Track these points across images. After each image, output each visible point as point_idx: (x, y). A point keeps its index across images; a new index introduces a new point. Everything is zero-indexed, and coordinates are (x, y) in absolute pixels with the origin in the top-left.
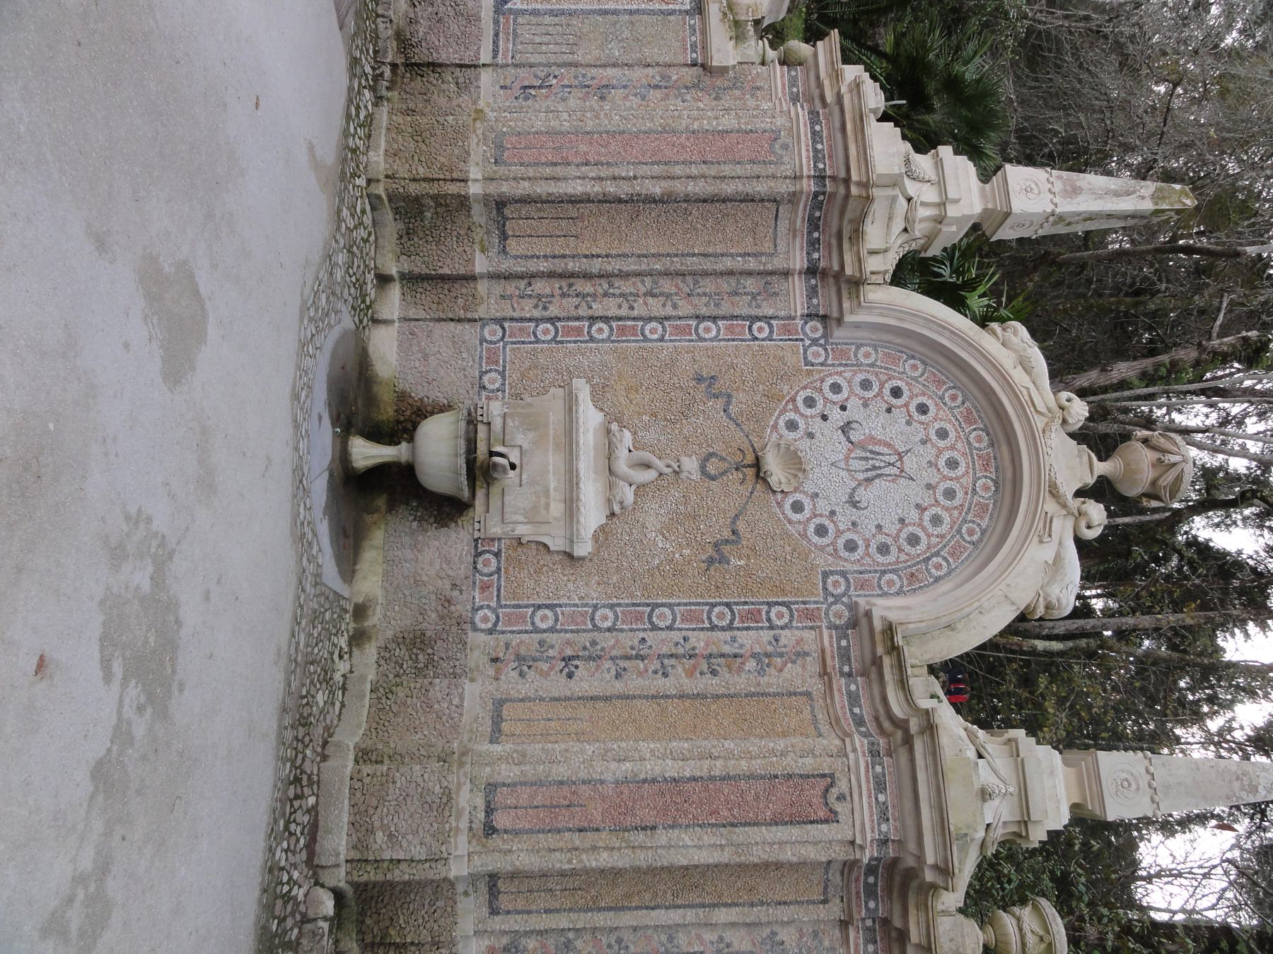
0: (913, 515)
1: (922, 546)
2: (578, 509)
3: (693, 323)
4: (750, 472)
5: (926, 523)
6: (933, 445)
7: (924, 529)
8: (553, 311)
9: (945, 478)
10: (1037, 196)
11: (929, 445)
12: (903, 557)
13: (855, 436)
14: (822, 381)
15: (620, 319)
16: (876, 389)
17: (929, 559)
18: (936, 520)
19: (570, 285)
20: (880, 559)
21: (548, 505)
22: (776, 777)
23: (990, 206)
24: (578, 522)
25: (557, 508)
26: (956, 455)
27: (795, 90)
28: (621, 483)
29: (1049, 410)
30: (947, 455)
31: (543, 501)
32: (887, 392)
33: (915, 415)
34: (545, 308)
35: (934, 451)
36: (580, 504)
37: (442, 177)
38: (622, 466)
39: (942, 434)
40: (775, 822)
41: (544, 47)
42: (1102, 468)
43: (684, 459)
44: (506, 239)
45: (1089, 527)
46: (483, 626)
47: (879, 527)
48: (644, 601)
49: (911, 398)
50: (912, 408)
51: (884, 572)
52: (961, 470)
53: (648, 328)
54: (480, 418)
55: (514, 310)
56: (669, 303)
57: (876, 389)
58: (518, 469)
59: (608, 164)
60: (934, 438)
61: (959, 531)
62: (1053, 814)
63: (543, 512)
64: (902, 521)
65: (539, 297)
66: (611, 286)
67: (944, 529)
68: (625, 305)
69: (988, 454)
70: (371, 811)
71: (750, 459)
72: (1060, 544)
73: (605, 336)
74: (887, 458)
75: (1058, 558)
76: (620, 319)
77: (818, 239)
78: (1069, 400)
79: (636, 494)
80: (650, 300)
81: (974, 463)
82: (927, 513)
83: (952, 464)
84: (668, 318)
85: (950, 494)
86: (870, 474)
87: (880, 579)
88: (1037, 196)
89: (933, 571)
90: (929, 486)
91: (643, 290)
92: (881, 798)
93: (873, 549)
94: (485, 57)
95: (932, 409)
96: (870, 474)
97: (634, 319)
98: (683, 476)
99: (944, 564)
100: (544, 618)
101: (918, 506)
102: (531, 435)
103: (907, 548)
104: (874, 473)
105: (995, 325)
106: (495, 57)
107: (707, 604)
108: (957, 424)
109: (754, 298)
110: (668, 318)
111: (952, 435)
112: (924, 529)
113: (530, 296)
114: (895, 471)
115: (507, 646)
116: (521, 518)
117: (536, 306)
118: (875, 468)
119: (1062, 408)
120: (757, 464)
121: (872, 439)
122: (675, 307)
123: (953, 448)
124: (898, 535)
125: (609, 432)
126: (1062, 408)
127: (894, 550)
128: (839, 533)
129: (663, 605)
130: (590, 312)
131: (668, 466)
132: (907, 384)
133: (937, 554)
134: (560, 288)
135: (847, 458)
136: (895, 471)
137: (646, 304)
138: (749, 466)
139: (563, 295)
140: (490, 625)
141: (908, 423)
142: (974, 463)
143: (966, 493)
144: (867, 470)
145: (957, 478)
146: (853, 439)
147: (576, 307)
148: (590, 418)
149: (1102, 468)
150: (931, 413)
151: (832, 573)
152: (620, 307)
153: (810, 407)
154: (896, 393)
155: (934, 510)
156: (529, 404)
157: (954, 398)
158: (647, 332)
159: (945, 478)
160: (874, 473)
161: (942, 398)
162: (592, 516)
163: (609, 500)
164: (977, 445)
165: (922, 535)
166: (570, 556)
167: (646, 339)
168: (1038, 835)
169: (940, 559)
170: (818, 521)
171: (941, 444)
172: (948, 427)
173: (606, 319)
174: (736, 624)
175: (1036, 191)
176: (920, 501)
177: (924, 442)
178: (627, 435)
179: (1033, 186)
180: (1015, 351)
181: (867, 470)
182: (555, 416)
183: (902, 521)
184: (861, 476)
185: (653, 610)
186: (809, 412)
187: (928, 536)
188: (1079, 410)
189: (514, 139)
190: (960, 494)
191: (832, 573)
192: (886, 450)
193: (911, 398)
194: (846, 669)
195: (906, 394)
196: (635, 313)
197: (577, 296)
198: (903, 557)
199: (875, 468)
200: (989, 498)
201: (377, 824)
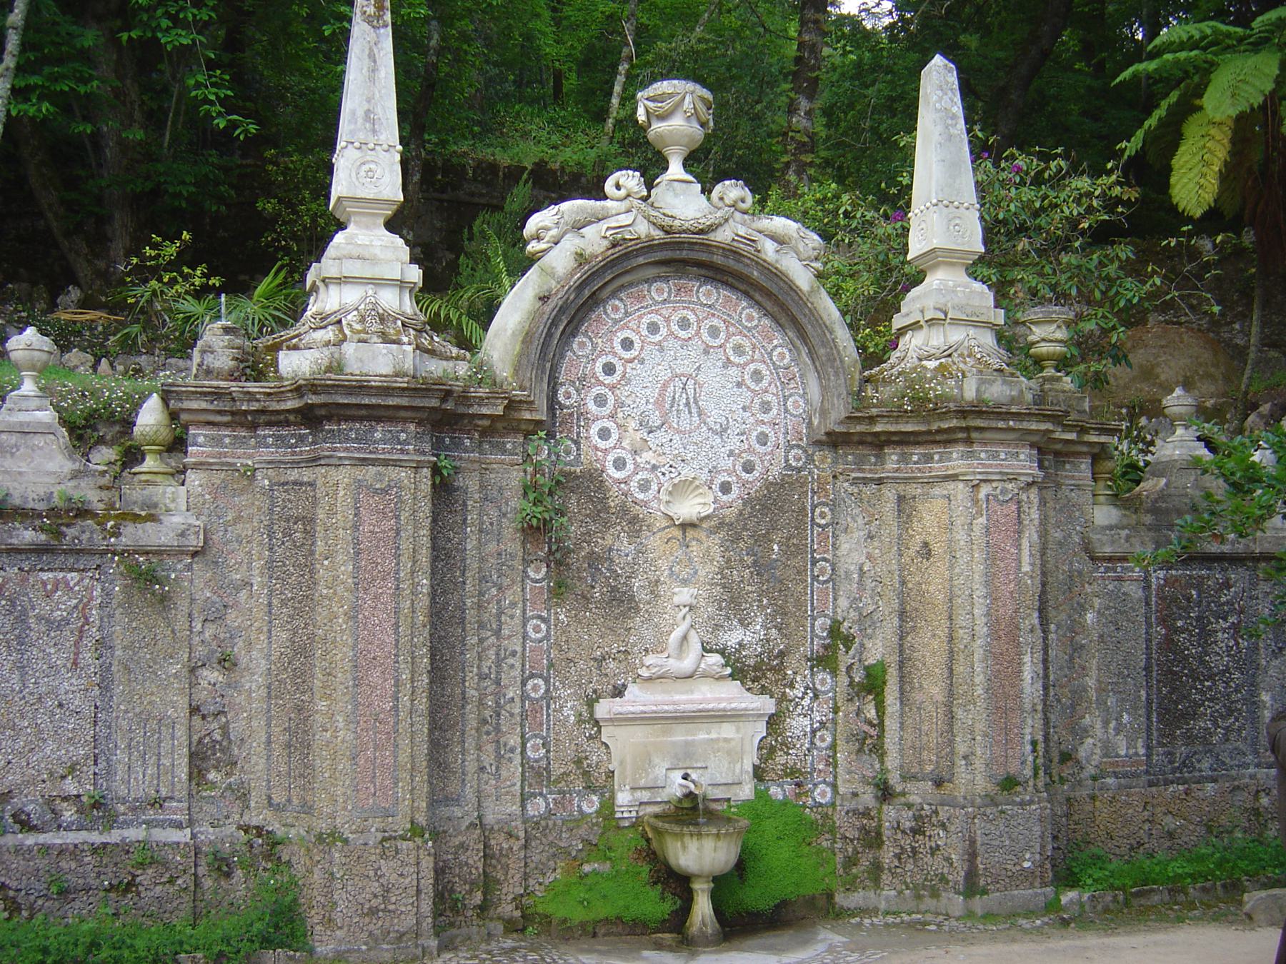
0: (733, 371)
1: (762, 367)
2: (733, 709)
3: (529, 584)
4: (691, 533)
5: (742, 360)
6: (665, 339)
7: (746, 364)
8: (514, 741)
9: (698, 333)
10: (368, 161)
11: (665, 344)
12: (773, 389)
13: (655, 420)
14: (597, 449)
15: (523, 666)
16: (604, 390)
17: (774, 364)
18: (738, 350)
19: (485, 722)
20: (774, 411)
21: (726, 740)
22: (988, 542)
23: (381, 221)
24: (746, 709)
25: (728, 730)
26: (675, 318)
27: (227, 440)
28: (702, 666)
29: (629, 211)
30: (675, 328)
31: (721, 744)
32: (608, 380)
33: (633, 353)
34: (512, 750)
35: (671, 340)
36: (728, 707)
37: (415, 876)
38: (687, 664)
39: (654, 328)
40: (1019, 547)
41: (163, 761)
42: (676, 169)
43: (676, 600)
44: (447, 798)
45: (743, 201)
46: (829, 795)
47: (744, 408)
48: (808, 644)
49: (615, 354)
50: (627, 355)
51: (786, 411)
52: (692, 317)
53: (532, 635)
54: (634, 814)
55: (514, 785)
56: (508, 611)
57: (604, 390)
58: (689, 771)
59: (396, 685)
60: (658, 338)
61: (749, 330)
62: (980, 296)
63: (733, 743)
64: (739, 385)
65: (499, 757)
66: (487, 676)
67: (746, 343)
68: (511, 661)
69: (675, 285)
70: (1010, 874)
71: (677, 533)
72: (760, 232)
73: (541, 682)
74: (679, 391)
75: (773, 237)
76: (523, 666)
77: (451, 438)
78: (618, 187)
79: (710, 651)
80: (505, 632)
81: (684, 302)
82: (732, 358)
83: (684, 324)
84: (524, 612)
85: (714, 332)
86: (694, 410)
87: (792, 415)
88: (368, 161)
89: (785, 361)
90: (706, 352)
91: (493, 640)
92: (1003, 456)
93: (766, 418)
94: (183, 836)
95: (627, 334)
96: (694, 410)
97: (524, 650)
98: (694, 602)
99: (779, 349)
100: (823, 740)
101: (725, 367)
102: (656, 760)
103: (765, 383)
104: (693, 405)
105: (533, 247)
106: (179, 826)
107: (812, 584)
108: (643, 311)
109: (505, 515)
110: (524, 612)
111: (655, 318)
112: (746, 364)
113: (497, 768)
114: (691, 382)
115: (849, 773)
116: (738, 766)
117: (510, 760)
118: (687, 404)
119: (629, 195)
120: (686, 526)
121: (659, 403)
122: (513, 605)
123: (667, 320)
124: (753, 391)
125: (650, 679)
126: (629, 195)
127: (769, 398)
128: (750, 450)
129: (813, 626)
130: (517, 700)
131: (684, 618)
132: (599, 356)
133: (770, 354)
134: (488, 733)
135: (678, 431)
136: (691, 382)
137: (510, 637)
138: (684, 533)
139: (497, 729)
140: (828, 790)
141: (642, 362)
142: (684, 302)
143: (713, 315)
144: (690, 412)
145: (698, 321)
146: (659, 422)
147: (512, 715)
148: (637, 698)
149: (676, 169)
150: (635, 338)
151: (787, 461)
152: (512, 666)
153: (624, 464)
154: (609, 369)
155: (730, 352)
156: (621, 763)
157: (616, 309)
158: (539, 636)
159: (698, 333)
160: (693, 405)
161: (616, 322)
162: (732, 695)
163: (722, 678)
164: (666, 295)
165: (752, 367)
166: (772, 716)
167: (547, 637)
168: (999, 317)
169: (775, 353)
170: (739, 468)
171: (664, 331)
172: (646, 320)
173: (524, 683)
174: (829, 557)
175: (373, 166)
176: (720, 364)
177: (662, 350)
178: (650, 660)
179: (366, 167)
180: (565, 233)
181: (690, 412)
182: (637, 735)
183: (739, 385)
184: (696, 418)
185: (817, 636)
186: (630, 467)
187: (753, 361)
188: (630, 180)
189: (362, 795)
190: (716, 322)
191: (787, 461)
192: (671, 389)
193: (615, 354)
194: (873, 460)
195: (610, 358)
196: (519, 649)
197: (499, 715)
198: (773, 389)
199: (687, 404)
200: (719, 293)
201: (1018, 868)
